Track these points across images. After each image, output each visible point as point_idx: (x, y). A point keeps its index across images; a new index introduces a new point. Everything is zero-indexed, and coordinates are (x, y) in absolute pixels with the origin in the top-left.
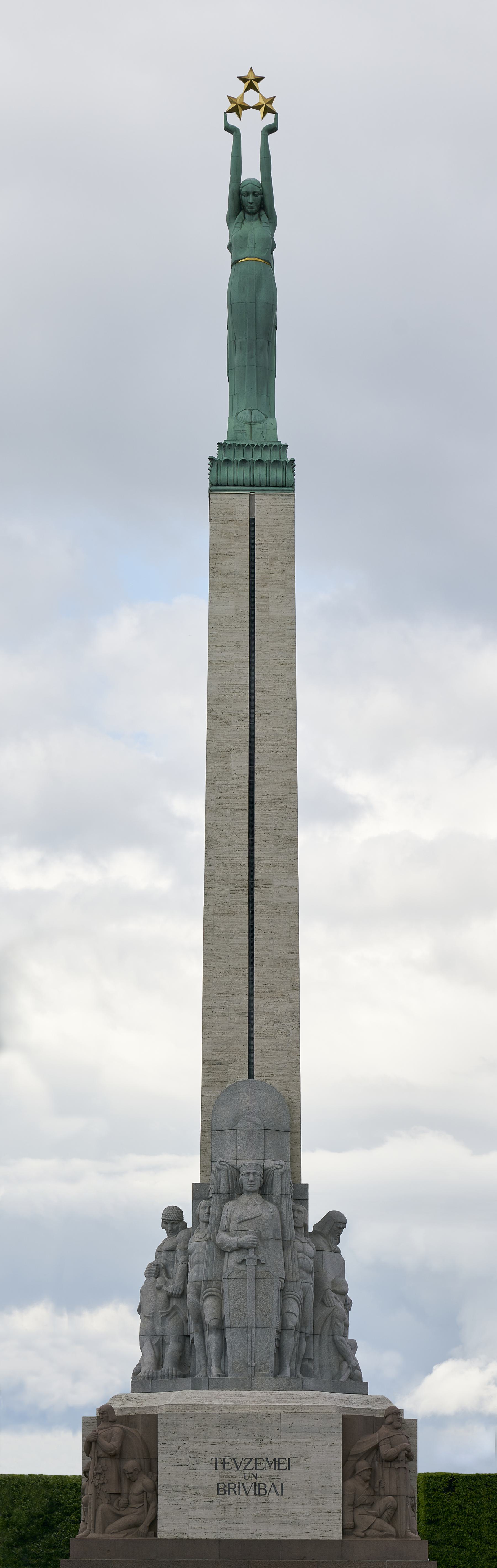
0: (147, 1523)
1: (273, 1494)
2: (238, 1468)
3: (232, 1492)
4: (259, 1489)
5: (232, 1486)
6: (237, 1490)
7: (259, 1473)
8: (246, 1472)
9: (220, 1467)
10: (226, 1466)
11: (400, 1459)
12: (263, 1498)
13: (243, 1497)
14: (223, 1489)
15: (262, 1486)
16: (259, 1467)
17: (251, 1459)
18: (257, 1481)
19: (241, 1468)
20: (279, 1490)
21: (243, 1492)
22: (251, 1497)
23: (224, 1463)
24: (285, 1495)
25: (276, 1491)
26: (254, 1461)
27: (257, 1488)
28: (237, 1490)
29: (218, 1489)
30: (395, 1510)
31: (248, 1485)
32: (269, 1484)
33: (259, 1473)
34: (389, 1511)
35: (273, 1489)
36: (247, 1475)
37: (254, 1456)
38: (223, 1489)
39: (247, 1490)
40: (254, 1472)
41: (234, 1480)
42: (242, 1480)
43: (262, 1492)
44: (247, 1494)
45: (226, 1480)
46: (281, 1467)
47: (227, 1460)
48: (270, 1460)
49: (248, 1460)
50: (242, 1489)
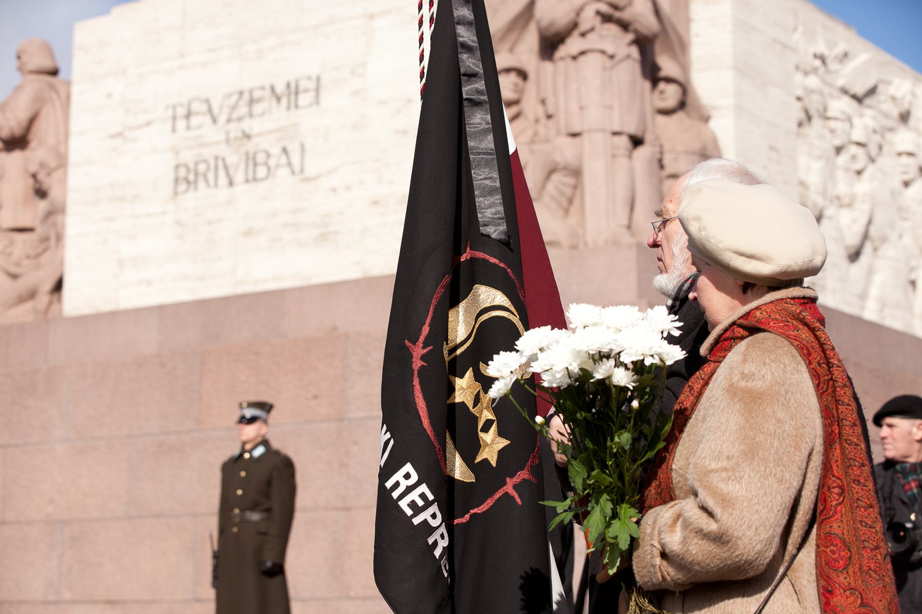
0: (49, 285)
1: (284, 172)
2: (215, 121)
3: (201, 184)
4: (255, 165)
5: (202, 168)
6: (211, 176)
7: (254, 126)
8: (233, 126)
9: (181, 124)
10: (195, 121)
11: (584, 26)
12: (261, 187)
13: (224, 192)
14: (187, 178)
15: (261, 158)
16: (258, 108)
17: (241, 93)
18: (250, 146)
19: (222, 119)
20: (296, 159)
21: (223, 180)
22: (240, 188)
23: (188, 116)
24: (310, 170)
25: (289, 164)
26: (246, 97)
27: (251, 161)
28: (211, 176)
29: (177, 180)
30: (577, 173)
31: (231, 159)
32: (275, 150)
33: (254, 126)
34: (556, 177)
35: (283, 160)
36: (232, 135)
37: (246, 85)
38: (187, 178)
39: (232, 172)
40: (247, 125)
41: (208, 153)
42: (223, 150)
43: (261, 172)
44: (231, 183)
45: (188, 157)
46: (304, 99)
47: (196, 106)
48: (280, 88)
49: (234, 98)
50: (222, 172)
